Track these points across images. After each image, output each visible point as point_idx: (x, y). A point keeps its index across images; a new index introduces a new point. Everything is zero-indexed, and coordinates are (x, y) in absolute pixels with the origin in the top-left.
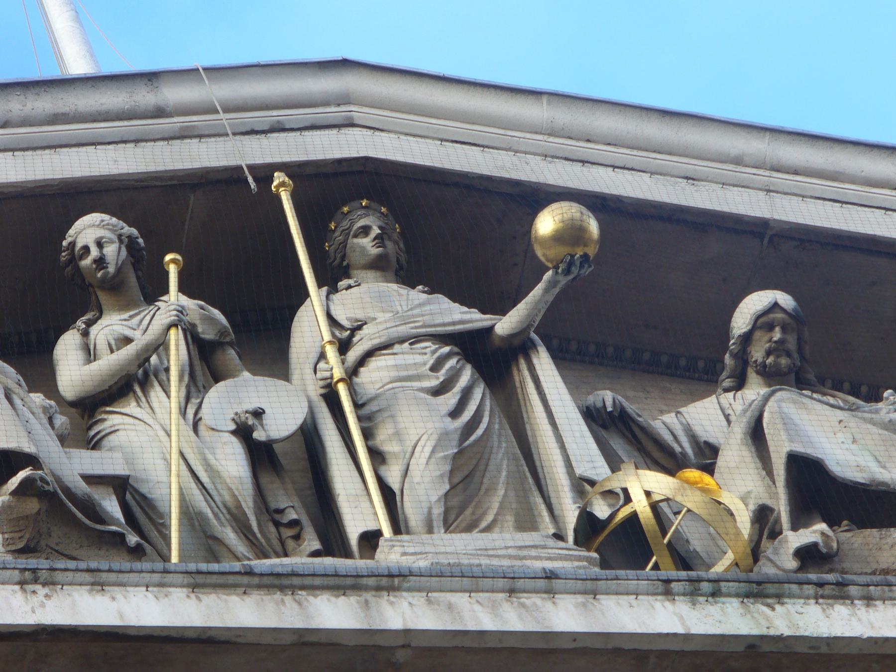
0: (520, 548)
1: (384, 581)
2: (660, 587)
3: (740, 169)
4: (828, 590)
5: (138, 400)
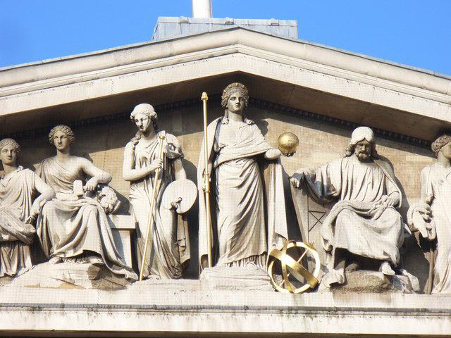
4: (331, 312)
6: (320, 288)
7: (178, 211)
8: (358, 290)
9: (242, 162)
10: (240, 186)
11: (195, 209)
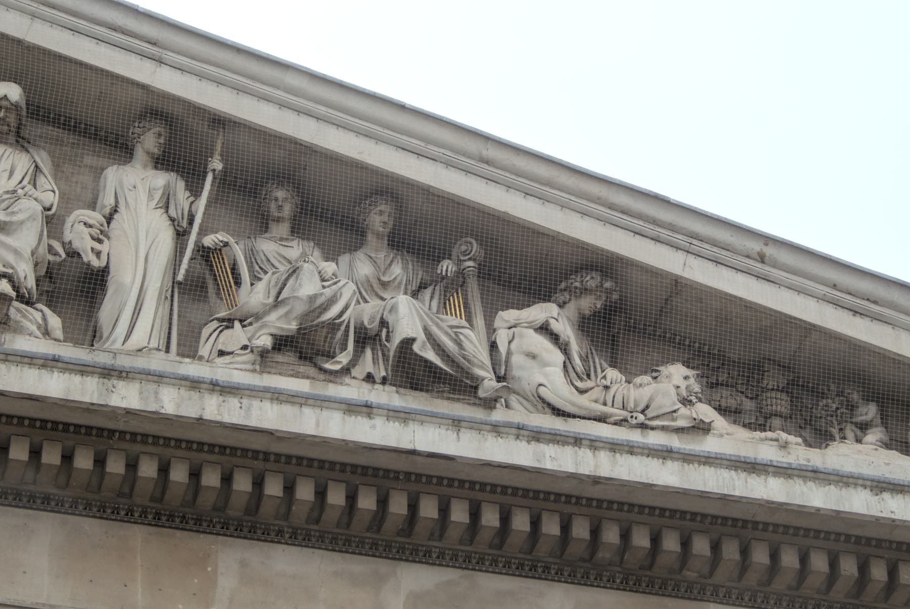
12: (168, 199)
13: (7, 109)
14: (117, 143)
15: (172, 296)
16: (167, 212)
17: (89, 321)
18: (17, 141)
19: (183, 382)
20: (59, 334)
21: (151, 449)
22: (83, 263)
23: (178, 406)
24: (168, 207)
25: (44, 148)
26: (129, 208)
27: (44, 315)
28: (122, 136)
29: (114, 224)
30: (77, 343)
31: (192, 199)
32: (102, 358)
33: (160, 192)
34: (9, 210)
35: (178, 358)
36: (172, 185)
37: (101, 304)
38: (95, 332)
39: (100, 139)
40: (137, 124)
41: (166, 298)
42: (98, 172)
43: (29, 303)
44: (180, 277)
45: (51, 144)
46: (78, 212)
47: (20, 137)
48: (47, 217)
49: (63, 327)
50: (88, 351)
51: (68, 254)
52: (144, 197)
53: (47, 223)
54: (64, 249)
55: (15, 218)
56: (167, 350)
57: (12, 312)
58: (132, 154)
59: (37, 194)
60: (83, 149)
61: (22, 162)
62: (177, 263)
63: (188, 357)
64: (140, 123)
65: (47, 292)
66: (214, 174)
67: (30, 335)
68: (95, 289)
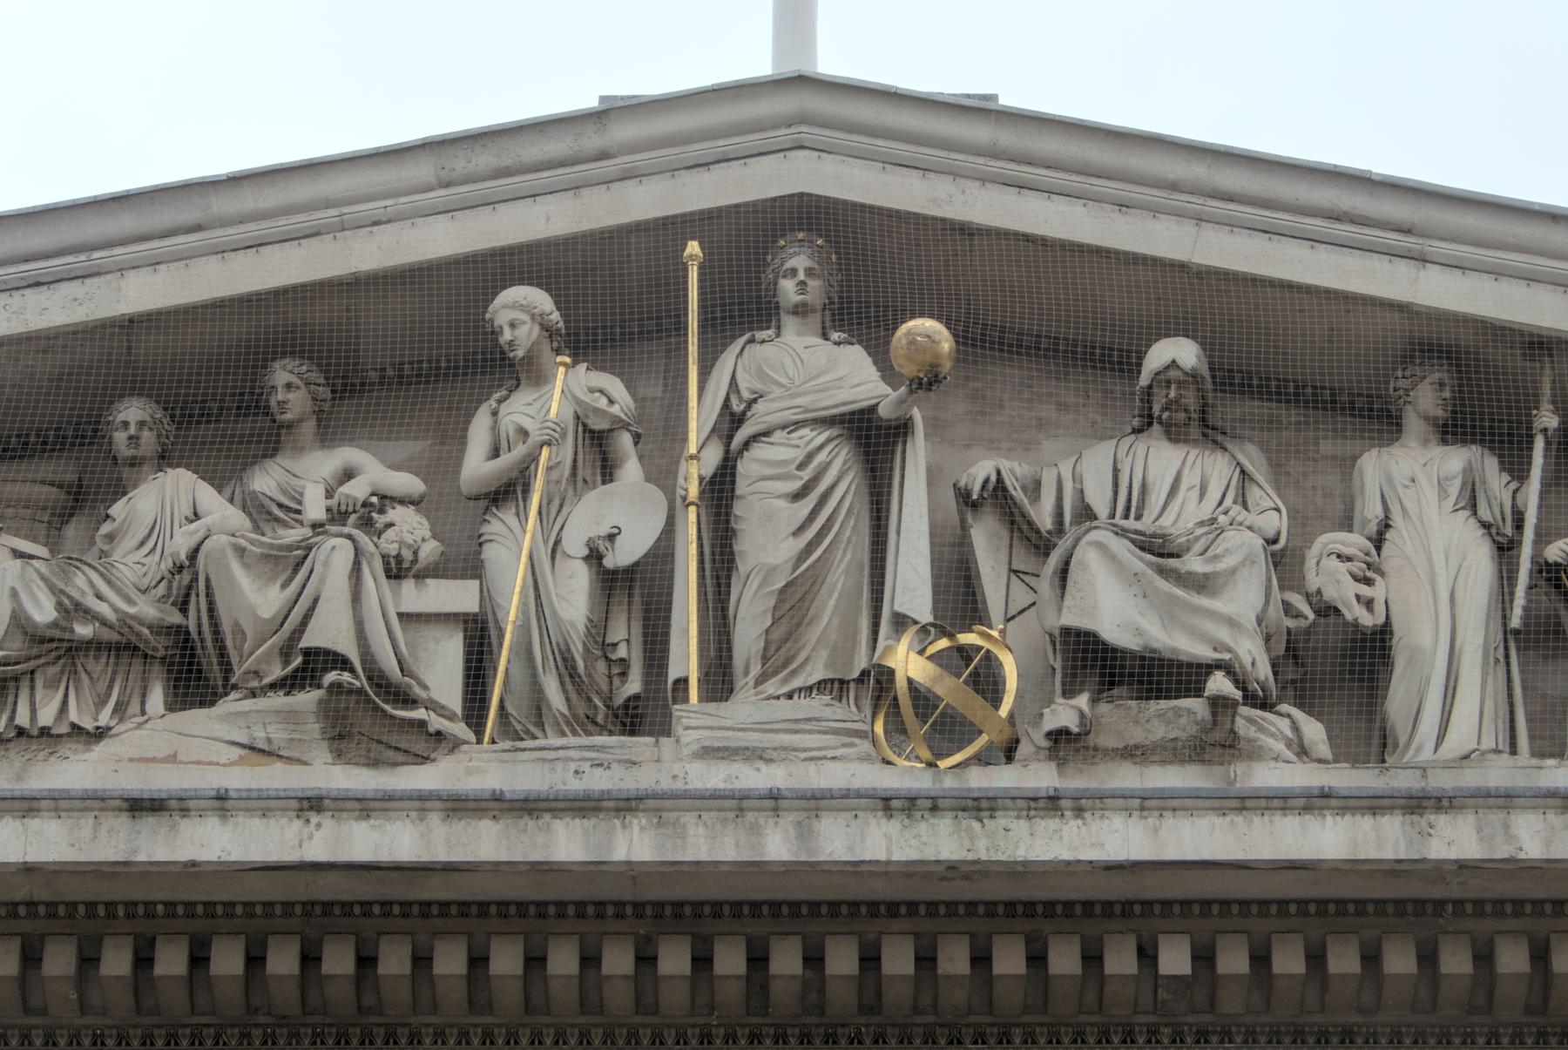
0: (797, 721)
1: (622, 804)
2: (880, 804)
3: (1177, 196)
5: (517, 506)
6: (1024, 749)
7: (609, 563)
8: (1133, 753)
9: (805, 431)
10: (797, 496)
11: (662, 554)
12: (1473, 490)
13: (1180, 383)
14: (1371, 410)
15: (1507, 656)
16: (1475, 513)
17: (1370, 721)
18: (1205, 435)
19: (1550, 801)
20: (1324, 750)
21: (1514, 924)
22: (1346, 624)
23: (1548, 842)
24: (1473, 506)
25: (1250, 440)
26: (1409, 516)
27: (1293, 722)
28: (1379, 397)
29: (1387, 548)
30: (1358, 762)
31: (1514, 485)
32: (1403, 781)
33: (1457, 484)
34: (1210, 553)
35: (1534, 761)
36: (1477, 466)
37: (1387, 688)
38: (1385, 737)
39: (1343, 409)
40: (1399, 373)
41: (1497, 661)
42: (1347, 465)
43: (1265, 705)
44: (1515, 622)
45: (1261, 429)
46: (1324, 538)
47: (1207, 426)
48: (1273, 555)
49: (1330, 738)
50: (1377, 771)
51: (1318, 612)
52: (1430, 493)
53: (1276, 565)
54: (1310, 604)
55: (1220, 566)
56: (1514, 750)
57: (1241, 726)
58: (1399, 425)
59: (1251, 519)
60: (1316, 429)
61: (1217, 469)
62: (1507, 597)
63: (1552, 756)
64: (1404, 369)
65: (1294, 681)
66: (1546, 436)
67: (1276, 759)
68: (1372, 664)
